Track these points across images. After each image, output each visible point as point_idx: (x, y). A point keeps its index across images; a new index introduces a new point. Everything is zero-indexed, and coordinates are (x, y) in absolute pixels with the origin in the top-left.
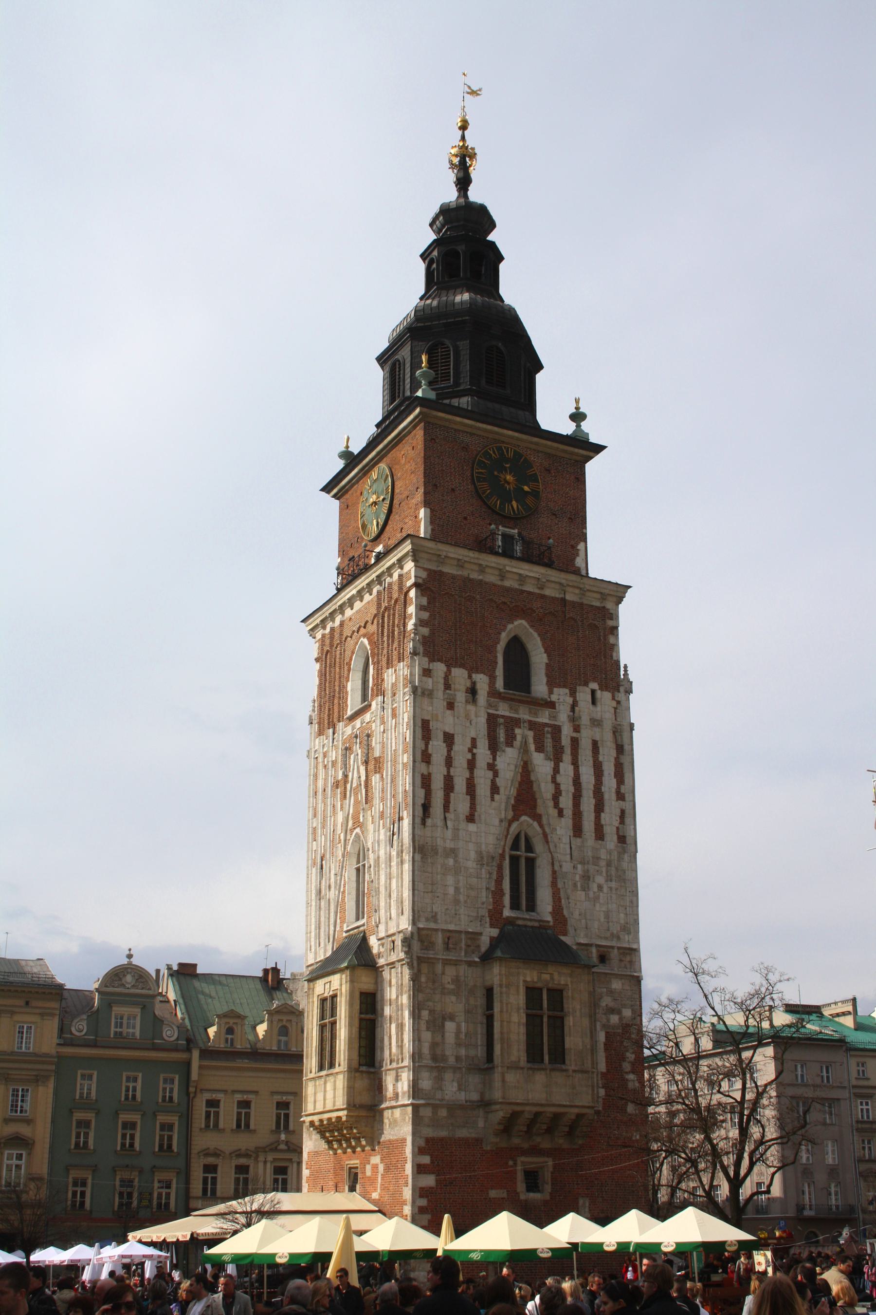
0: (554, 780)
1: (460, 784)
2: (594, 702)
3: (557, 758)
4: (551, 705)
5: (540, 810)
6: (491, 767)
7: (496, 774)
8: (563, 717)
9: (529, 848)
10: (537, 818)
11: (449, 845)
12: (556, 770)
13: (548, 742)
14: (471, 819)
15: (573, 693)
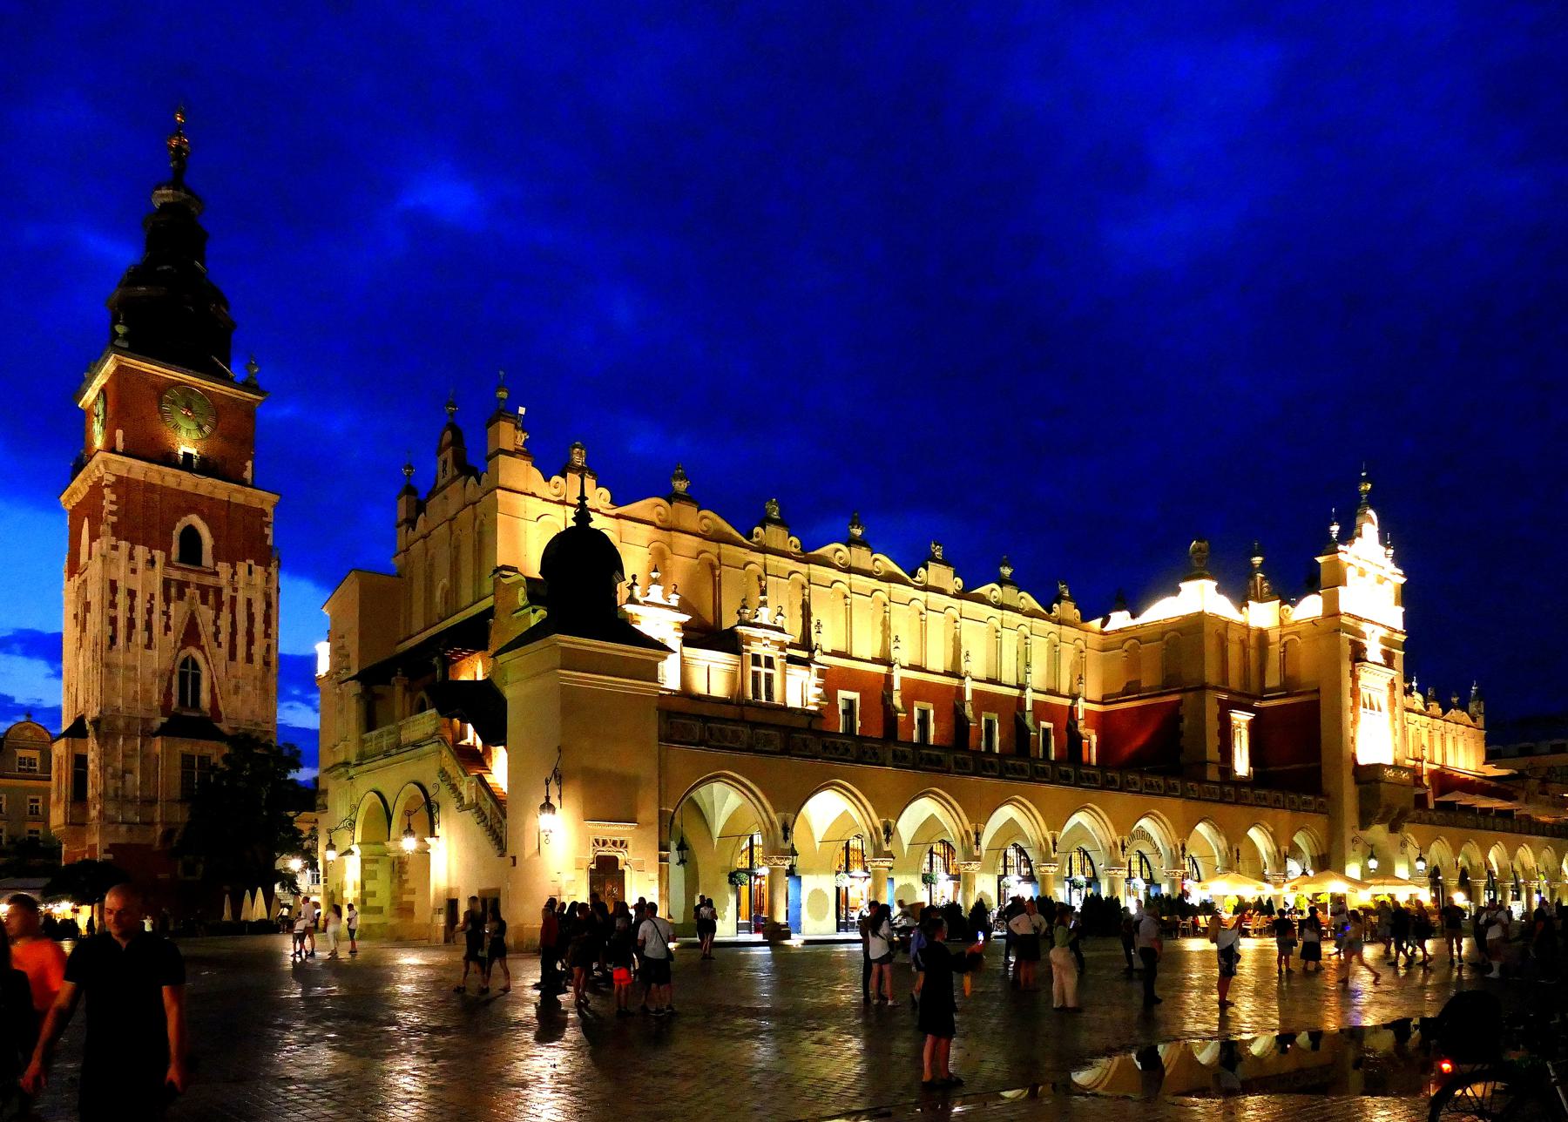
0: (215, 623)
1: (140, 624)
2: (250, 573)
3: (218, 607)
4: (216, 574)
5: (204, 641)
6: (166, 613)
7: (169, 618)
8: (224, 580)
9: (195, 666)
10: (201, 648)
11: (131, 663)
12: (217, 617)
13: (211, 598)
14: (149, 646)
15: (234, 566)
